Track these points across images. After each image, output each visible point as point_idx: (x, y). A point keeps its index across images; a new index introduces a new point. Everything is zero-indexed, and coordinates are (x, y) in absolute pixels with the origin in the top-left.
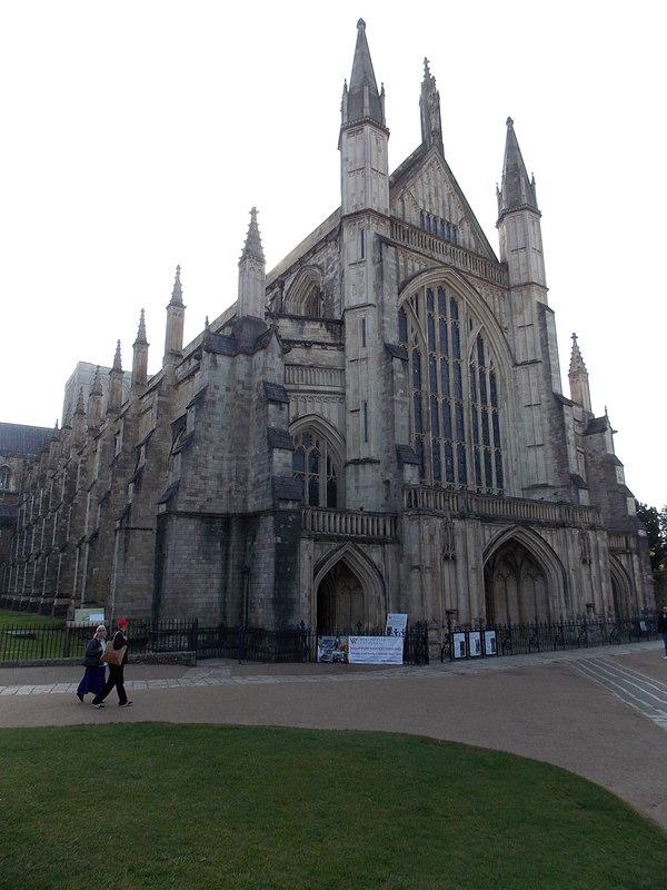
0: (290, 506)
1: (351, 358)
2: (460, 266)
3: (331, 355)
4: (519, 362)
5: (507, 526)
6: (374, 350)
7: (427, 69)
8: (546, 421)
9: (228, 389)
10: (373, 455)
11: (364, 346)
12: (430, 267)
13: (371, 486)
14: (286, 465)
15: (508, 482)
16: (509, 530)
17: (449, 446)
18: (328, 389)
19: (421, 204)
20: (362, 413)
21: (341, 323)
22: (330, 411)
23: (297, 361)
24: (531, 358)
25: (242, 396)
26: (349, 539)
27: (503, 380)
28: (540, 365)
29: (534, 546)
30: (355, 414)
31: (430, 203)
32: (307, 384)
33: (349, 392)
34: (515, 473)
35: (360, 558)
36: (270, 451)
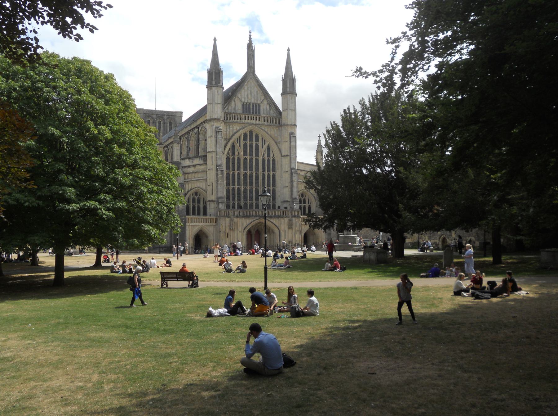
2: (257, 122)
3: (203, 167)
4: (283, 155)
6: (214, 167)
7: (250, 36)
8: (289, 178)
10: (214, 199)
12: (243, 126)
18: (202, 178)
19: (243, 100)
20: (211, 186)
21: (206, 156)
22: (202, 185)
23: (191, 171)
24: (286, 154)
27: (278, 162)
28: (289, 157)
31: (248, 97)
34: (279, 196)
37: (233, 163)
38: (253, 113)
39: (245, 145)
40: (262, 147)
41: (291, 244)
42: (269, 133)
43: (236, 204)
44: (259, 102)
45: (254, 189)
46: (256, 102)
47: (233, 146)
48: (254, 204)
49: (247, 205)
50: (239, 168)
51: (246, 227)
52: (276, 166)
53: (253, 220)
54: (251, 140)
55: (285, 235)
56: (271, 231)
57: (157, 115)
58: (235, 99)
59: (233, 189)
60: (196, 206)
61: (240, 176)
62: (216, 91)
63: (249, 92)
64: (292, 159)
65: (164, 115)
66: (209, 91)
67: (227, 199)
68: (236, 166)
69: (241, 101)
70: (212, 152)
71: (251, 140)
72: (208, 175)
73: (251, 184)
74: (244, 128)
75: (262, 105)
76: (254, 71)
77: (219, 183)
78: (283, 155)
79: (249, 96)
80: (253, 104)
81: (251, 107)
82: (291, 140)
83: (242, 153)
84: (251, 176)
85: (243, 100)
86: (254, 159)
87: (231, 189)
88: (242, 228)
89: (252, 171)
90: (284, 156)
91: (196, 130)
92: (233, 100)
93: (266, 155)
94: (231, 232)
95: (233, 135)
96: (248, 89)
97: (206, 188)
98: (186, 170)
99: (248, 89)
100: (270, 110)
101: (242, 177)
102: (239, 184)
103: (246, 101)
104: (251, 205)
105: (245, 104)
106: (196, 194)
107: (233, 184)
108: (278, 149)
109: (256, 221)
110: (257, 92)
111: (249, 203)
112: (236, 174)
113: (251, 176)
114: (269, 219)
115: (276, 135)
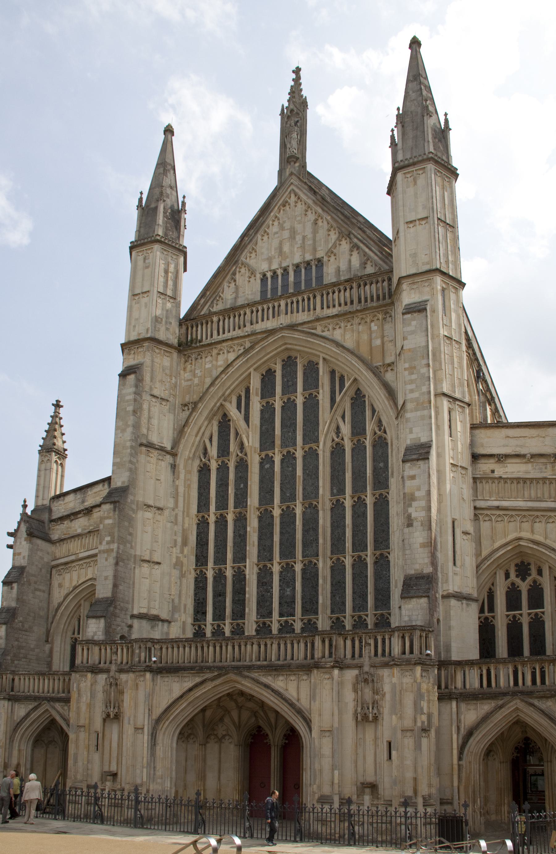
2: (302, 317)
37: (223, 484)
63: (286, 234)
80: (297, 266)
85: (264, 267)
92: (229, 276)
96: (282, 228)
99: (282, 228)
103: (275, 266)
107: (220, 559)
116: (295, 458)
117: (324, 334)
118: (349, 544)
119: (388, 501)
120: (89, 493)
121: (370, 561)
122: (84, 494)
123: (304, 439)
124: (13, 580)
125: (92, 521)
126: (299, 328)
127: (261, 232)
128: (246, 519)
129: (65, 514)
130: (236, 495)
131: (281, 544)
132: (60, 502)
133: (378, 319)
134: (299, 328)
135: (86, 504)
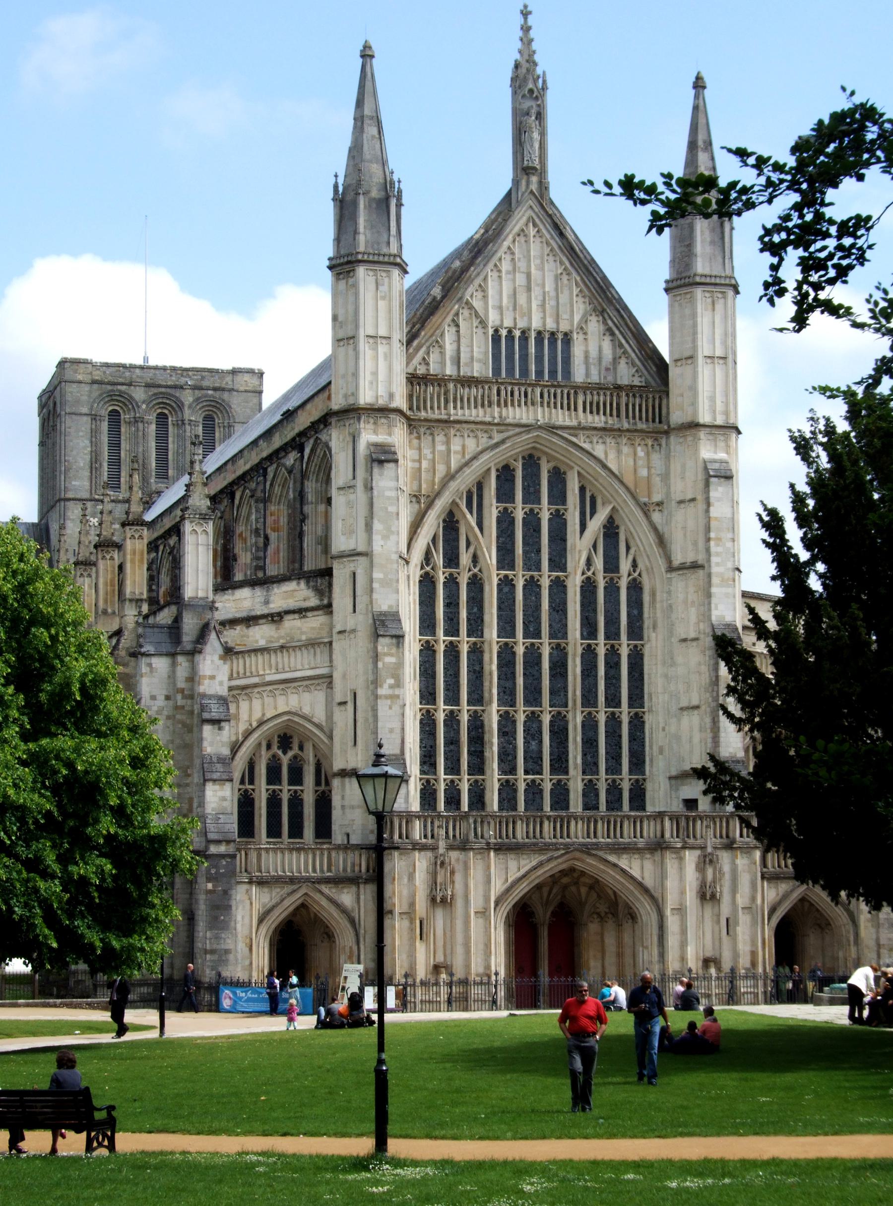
0: (222, 849)
1: (338, 628)
2: (561, 418)
3: (314, 624)
4: (676, 563)
5: (550, 854)
6: (361, 622)
7: (526, 29)
8: (704, 669)
9: (168, 698)
11: (354, 611)
12: (497, 438)
13: (359, 807)
14: (224, 799)
15: (651, 766)
16: (550, 860)
17: (533, 719)
19: (493, 318)
21: (328, 573)
23: (262, 643)
24: (690, 558)
25: (183, 707)
26: (308, 880)
27: (653, 594)
28: (701, 572)
29: (610, 877)
30: (342, 708)
32: (278, 672)
33: (337, 676)
35: (324, 902)
36: (204, 785)
38: (540, 373)
39: (506, 522)
40: (583, 528)
41: (713, 971)
42: (613, 466)
43: (465, 787)
44: (564, 327)
45: (546, 719)
46: (550, 325)
47: (451, 524)
48: (547, 787)
49: (515, 791)
50: (476, 625)
51: (508, 891)
52: (646, 615)
53: (543, 858)
54: (531, 495)
55: (684, 931)
56: (621, 908)
57: (148, 386)
58: (457, 314)
59: (452, 720)
60: (285, 797)
61: (481, 662)
62: (371, 280)
63: (521, 279)
64: (715, 580)
65: (181, 387)
66: (342, 284)
67: (423, 763)
68: (463, 614)
69: (483, 323)
70: (355, 554)
71: (531, 495)
72: (337, 656)
73: (533, 696)
74: (497, 445)
75: (577, 339)
76: (543, 187)
77: (383, 691)
78: (676, 563)
79: (522, 299)
80: (539, 333)
81: (532, 349)
82: (713, 494)
83: (491, 557)
84: (533, 658)
86: (545, 583)
87: (441, 717)
88: (487, 899)
89: (538, 635)
90: (683, 567)
91: (291, 459)
92: (449, 319)
93: (599, 563)
94: (440, 913)
95: (450, 477)
97: (330, 716)
98: (232, 636)
100: (615, 361)
101: (492, 666)
102: (477, 697)
103: (508, 323)
104: (534, 790)
105: (504, 333)
106: (285, 742)
107: (453, 697)
108: (652, 538)
109: (554, 863)
110: (557, 278)
111: (522, 779)
112: (464, 649)
113: (533, 658)
114: (612, 858)
115: (644, 472)
116: (539, 586)
117: (586, 446)
118: (601, 698)
119: (642, 655)
120: (276, 590)
121: (625, 720)
122: (267, 591)
123: (549, 565)
124: (222, 717)
125: (282, 632)
126: (559, 432)
127: (491, 265)
128: (482, 652)
129: (238, 615)
130: (468, 620)
131: (525, 688)
132: (226, 597)
133: (646, 445)
134: (559, 432)
135: (272, 606)
